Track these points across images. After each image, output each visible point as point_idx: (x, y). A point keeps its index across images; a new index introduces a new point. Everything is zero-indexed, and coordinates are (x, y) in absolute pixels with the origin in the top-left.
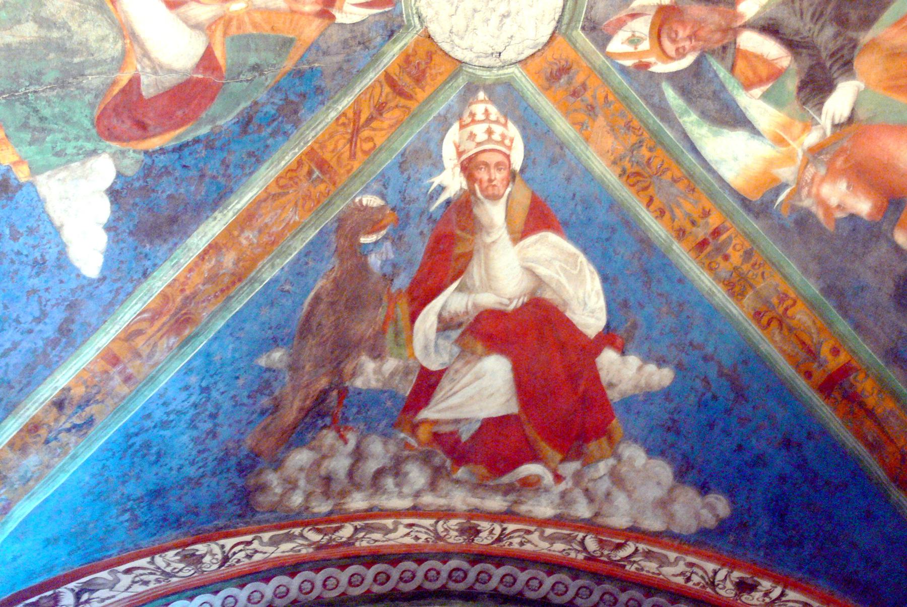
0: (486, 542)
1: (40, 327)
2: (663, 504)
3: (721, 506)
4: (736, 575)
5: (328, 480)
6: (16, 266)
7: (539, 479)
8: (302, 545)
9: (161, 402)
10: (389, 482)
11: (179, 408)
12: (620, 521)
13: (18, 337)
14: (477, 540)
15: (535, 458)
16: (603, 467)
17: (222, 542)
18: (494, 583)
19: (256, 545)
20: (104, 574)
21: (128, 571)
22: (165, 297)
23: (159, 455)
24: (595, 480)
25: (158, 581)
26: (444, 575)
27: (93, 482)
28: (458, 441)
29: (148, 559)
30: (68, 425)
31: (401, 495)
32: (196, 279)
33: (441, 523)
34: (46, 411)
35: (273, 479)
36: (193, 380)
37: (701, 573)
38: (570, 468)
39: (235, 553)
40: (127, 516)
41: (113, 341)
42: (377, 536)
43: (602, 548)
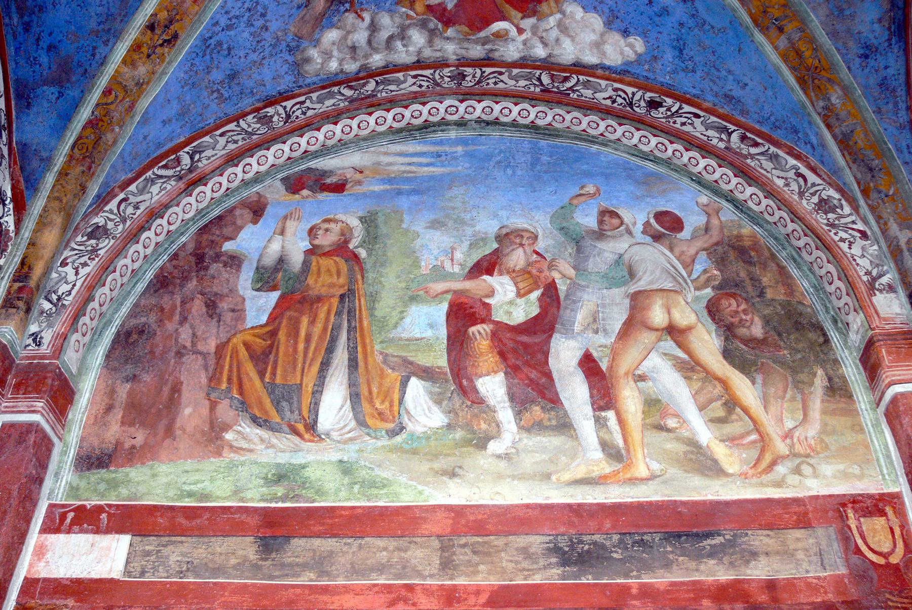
0: (471, 84)
2: (597, 45)
3: (639, 45)
4: (648, 95)
5: (354, 48)
7: (507, 32)
9: (223, 12)
10: (398, 44)
11: (237, 13)
14: (464, 83)
15: (504, 18)
16: (552, 21)
17: (284, 104)
18: (478, 112)
19: (308, 104)
21: (222, 135)
23: (229, 49)
24: (547, 30)
26: (442, 111)
27: (187, 77)
28: (445, 9)
29: (235, 123)
30: (160, 42)
33: (438, 72)
34: (143, 34)
35: (314, 53)
37: (623, 95)
38: (528, 23)
39: (294, 112)
40: (215, 95)
43: (553, 81)
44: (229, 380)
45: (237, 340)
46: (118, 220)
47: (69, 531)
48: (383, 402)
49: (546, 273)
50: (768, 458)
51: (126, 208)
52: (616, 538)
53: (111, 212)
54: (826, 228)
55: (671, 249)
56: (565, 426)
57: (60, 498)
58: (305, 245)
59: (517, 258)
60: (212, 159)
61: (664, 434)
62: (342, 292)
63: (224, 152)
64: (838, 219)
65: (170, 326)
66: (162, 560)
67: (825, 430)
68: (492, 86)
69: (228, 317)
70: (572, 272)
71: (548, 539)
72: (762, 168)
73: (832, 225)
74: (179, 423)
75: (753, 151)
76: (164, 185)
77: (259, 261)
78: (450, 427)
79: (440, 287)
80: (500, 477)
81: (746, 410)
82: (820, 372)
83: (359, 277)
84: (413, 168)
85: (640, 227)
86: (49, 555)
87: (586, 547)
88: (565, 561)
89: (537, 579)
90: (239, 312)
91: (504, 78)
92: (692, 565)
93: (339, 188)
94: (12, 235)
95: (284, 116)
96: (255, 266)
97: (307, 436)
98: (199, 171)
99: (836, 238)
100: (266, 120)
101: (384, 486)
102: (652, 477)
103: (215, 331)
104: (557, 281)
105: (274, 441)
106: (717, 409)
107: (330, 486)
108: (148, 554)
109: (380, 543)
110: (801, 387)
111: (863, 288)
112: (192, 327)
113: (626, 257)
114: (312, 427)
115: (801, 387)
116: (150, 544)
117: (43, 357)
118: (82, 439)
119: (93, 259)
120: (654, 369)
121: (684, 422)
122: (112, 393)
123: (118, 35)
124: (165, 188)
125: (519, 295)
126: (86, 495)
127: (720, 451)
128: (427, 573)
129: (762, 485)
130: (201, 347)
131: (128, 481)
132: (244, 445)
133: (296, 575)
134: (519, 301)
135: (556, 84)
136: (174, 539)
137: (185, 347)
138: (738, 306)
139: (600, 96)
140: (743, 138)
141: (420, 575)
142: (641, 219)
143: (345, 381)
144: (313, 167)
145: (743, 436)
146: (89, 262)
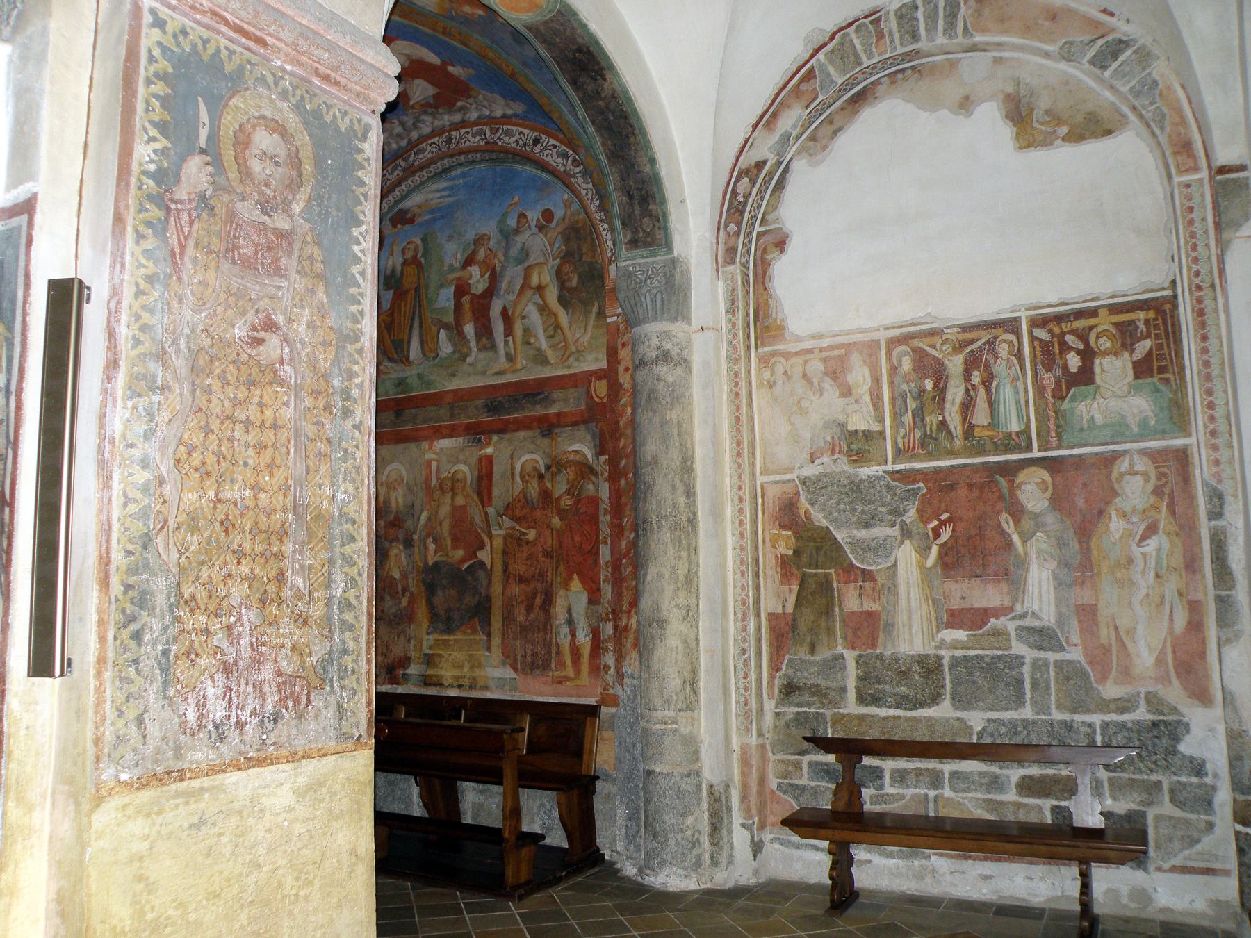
5: (399, 136)
50: (567, 353)
55: (546, 236)
56: (493, 347)
58: (401, 260)
59: (481, 254)
62: (415, 286)
70: (502, 258)
73: (602, 221)
78: (454, 352)
82: (596, 304)
84: (442, 200)
109: (432, 408)
110: (587, 313)
114: (408, 359)
121: (537, 339)
125: (482, 276)
127: (550, 354)
134: (481, 280)
145: (558, 344)
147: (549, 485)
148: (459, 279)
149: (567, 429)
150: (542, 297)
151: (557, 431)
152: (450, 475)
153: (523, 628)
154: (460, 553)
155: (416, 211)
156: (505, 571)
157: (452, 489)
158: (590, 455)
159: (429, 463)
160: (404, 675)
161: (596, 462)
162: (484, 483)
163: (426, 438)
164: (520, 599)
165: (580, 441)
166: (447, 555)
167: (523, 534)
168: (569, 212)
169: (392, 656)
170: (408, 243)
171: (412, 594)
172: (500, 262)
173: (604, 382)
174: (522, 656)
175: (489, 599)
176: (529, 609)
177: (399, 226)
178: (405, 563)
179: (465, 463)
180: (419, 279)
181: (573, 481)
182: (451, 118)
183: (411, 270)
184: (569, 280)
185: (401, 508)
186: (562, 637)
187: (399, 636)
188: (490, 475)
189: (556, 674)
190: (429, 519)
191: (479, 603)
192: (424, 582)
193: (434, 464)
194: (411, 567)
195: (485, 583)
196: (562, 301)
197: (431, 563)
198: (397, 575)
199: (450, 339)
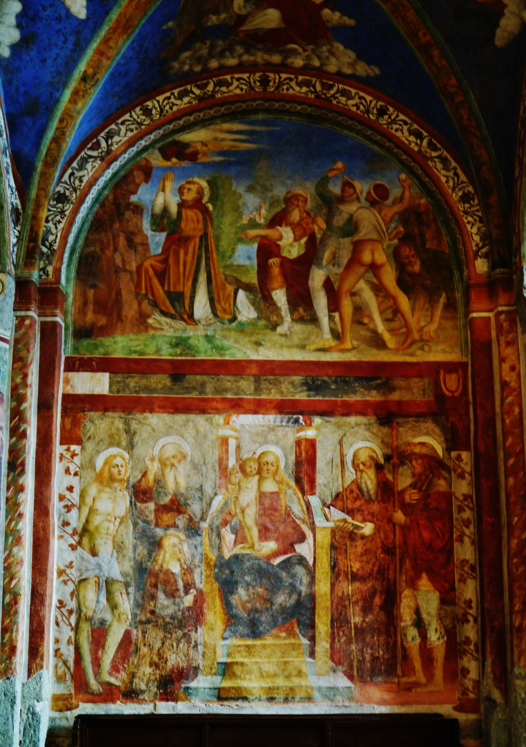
1: (67, 45)
2: (352, 65)
3: (377, 71)
6: (49, 21)
8: (193, 98)
12: (332, 68)
13: (58, 51)
17: (157, 98)
19: (172, 100)
20: (113, 126)
21: (123, 123)
22: (118, 21)
25: (136, 129)
29: (129, 114)
31: (233, 57)
32: (130, 10)
33: (252, 76)
34: (79, 84)
36: (135, 44)
38: (310, 47)
39: (165, 106)
41: (99, 45)
42: (224, 89)
44: (146, 289)
45: (147, 264)
46: (71, 189)
47: (78, 371)
48: (225, 303)
49: (311, 226)
50: (409, 341)
51: (74, 180)
52: (333, 378)
53: (66, 183)
54: (462, 214)
55: (380, 213)
56: (314, 320)
57: (69, 353)
59: (295, 215)
60: (120, 144)
61: (361, 326)
62: (201, 233)
63: (125, 139)
64: (470, 208)
65: (109, 253)
66: (127, 386)
67: (440, 328)
68: (285, 91)
69: (140, 249)
70: (324, 226)
71: (302, 378)
72: (436, 168)
73: (466, 212)
74: (124, 313)
75: (434, 154)
76: (94, 164)
77: (152, 210)
78: (259, 318)
79: (253, 233)
80: (282, 346)
81: (403, 316)
82: (444, 295)
83: (209, 224)
84: (237, 144)
85: (364, 194)
86: (71, 383)
87: (320, 383)
88: (309, 389)
89: (298, 397)
90: (145, 245)
91: (293, 84)
92: (366, 392)
93: (193, 157)
94: (21, 211)
95: (158, 109)
96: (150, 213)
97: (189, 322)
98: (113, 153)
99: (466, 221)
100: (147, 112)
101: (228, 349)
102: (354, 348)
103: (133, 257)
104: (316, 231)
105: (173, 324)
106: (389, 314)
107: (202, 349)
108: (119, 382)
109: (228, 378)
110: (432, 302)
111: (471, 254)
112: (121, 254)
113: (355, 216)
114: (191, 316)
115: (432, 302)
116: (119, 378)
117: (51, 283)
118: (74, 322)
119: (63, 218)
120: (361, 290)
121: (372, 319)
122: (84, 295)
123: (65, 85)
124: (95, 166)
125: (296, 240)
126: (83, 352)
127: (387, 336)
128: (248, 393)
129: (404, 355)
130: (128, 267)
131: (103, 345)
132: (157, 325)
133: (190, 393)
134: (296, 244)
135: (324, 91)
136: (131, 375)
137: (119, 267)
138: (410, 251)
139: (351, 102)
140: (430, 144)
141: (245, 394)
142: (366, 189)
143: (206, 291)
144: (177, 139)
145: (399, 329)
146: (61, 220)
147: (390, 477)
148: (263, 237)
149: (411, 419)
150: (377, 276)
151: (400, 420)
152: (257, 456)
153: (360, 631)
154: (271, 546)
155: (199, 147)
156: (333, 568)
157: (259, 472)
158: (440, 451)
159: (225, 441)
160: (187, 689)
161: (446, 456)
162: (305, 467)
163: (218, 411)
164: (354, 599)
165: (427, 434)
166: (252, 547)
167: (357, 527)
168: (407, 194)
169: (169, 665)
170: (189, 183)
171: (200, 593)
172: (320, 228)
173: (454, 377)
174: (359, 661)
175: (312, 597)
176: (366, 610)
177: (174, 160)
178: (188, 556)
179: (277, 443)
180: (206, 227)
181: (420, 475)
182: (266, 57)
183: (190, 214)
184: (410, 263)
185: (182, 490)
186: (409, 638)
187: (179, 641)
188: (312, 461)
189: (404, 680)
190: (226, 504)
191: (298, 603)
192: (217, 579)
193: (232, 443)
194: (197, 561)
195: (306, 580)
196: (401, 283)
197: (227, 555)
198: (176, 569)
199: (253, 303)
